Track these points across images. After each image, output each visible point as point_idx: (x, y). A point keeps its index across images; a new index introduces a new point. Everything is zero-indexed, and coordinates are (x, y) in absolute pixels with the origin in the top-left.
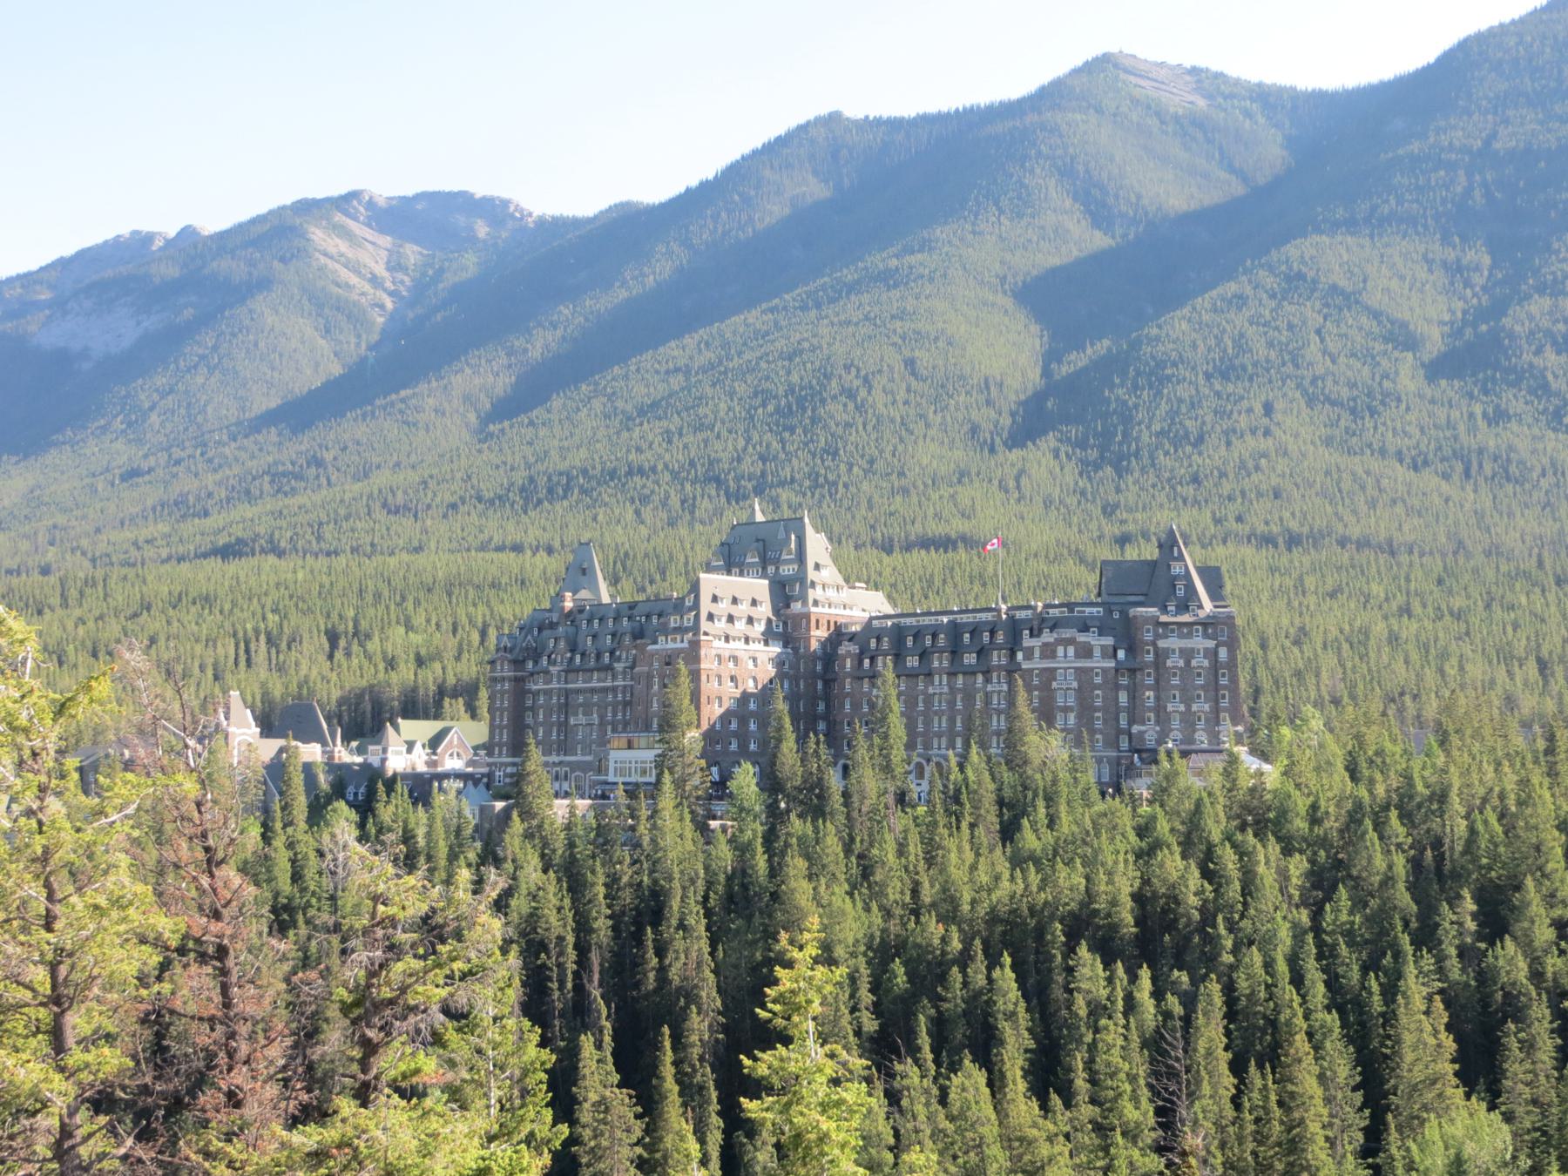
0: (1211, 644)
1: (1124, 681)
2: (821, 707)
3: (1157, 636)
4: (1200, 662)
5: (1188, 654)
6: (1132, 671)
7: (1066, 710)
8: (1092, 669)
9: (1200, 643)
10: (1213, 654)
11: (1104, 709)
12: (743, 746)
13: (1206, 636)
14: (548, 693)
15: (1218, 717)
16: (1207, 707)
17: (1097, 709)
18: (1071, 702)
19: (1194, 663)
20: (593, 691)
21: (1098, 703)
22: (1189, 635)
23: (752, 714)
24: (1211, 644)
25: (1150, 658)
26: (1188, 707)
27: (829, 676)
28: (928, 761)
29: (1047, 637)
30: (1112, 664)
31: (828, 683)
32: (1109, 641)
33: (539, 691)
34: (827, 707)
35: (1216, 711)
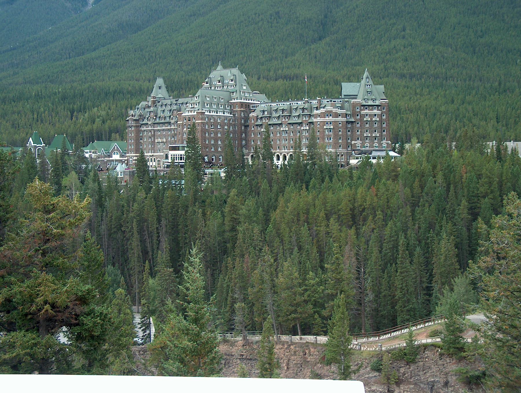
0: (379, 112)
1: (349, 126)
2: (244, 135)
3: (361, 110)
9: (375, 111)
10: (381, 116)
12: (216, 149)
14: (147, 131)
15: (382, 138)
16: (378, 135)
18: (331, 133)
20: (163, 130)
24: (379, 112)
26: (371, 134)
28: (281, 154)
29: (322, 110)
30: (344, 119)
31: (246, 126)
33: (145, 130)
35: (381, 135)
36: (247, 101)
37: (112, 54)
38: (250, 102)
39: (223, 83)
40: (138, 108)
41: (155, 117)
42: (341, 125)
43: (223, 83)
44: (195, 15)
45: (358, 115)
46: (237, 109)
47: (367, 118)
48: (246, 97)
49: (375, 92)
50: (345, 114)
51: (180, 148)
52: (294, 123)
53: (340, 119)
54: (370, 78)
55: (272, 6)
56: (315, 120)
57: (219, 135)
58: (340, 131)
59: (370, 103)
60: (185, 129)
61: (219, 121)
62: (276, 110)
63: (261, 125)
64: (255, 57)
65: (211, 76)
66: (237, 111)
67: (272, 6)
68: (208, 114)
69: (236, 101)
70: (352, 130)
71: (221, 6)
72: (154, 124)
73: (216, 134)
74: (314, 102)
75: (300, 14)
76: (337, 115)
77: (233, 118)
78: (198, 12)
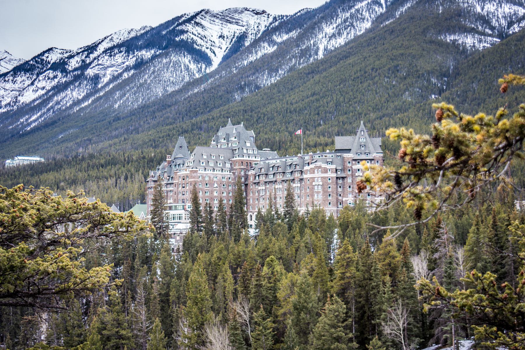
1: (340, 181)
3: (352, 164)
7: (318, 193)
8: (327, 177)
25: (350, 173)
27: (246, 183)
29: (312, 166)
30: (334, 175)
31: (246, 185)
32: (334, 167)
34: (246, 194)
36: (250, 159)
37: (222, 116)
38: (254, 159)
39: (228, 141)
40: (158, 169)
41: (168, 178)
42: (330, 181)
43: (228, 141)
44: (313, 72)
45: (349, 170)
46: (237, 167)
48: (249, 154)
49: (370, 145)
50: (335, 170)
51: (173, 208)
52: (287, 180)
53: (330, 175)
54: (365, 131)
55: (391, 59)
56: (305, 176)
57: (215, 194)
58: (329, 187)
59: (363, 157)
60: (180, 188)
61: (215, 179)
62: (273, 167)
63: (259, 183)
64: (365, 115)
65: (220, 134)
66: (236, 169)
67: (391, 59)
68: (203, 172)
69: (237, 158)
70: (343, 186)
71: (341, 62)
72: (167, 184)
73: (212, 192)
74: (307, 158)
75: (421, 67)
76: (325, 171)
77: (232, 176)
78: (317, 70)
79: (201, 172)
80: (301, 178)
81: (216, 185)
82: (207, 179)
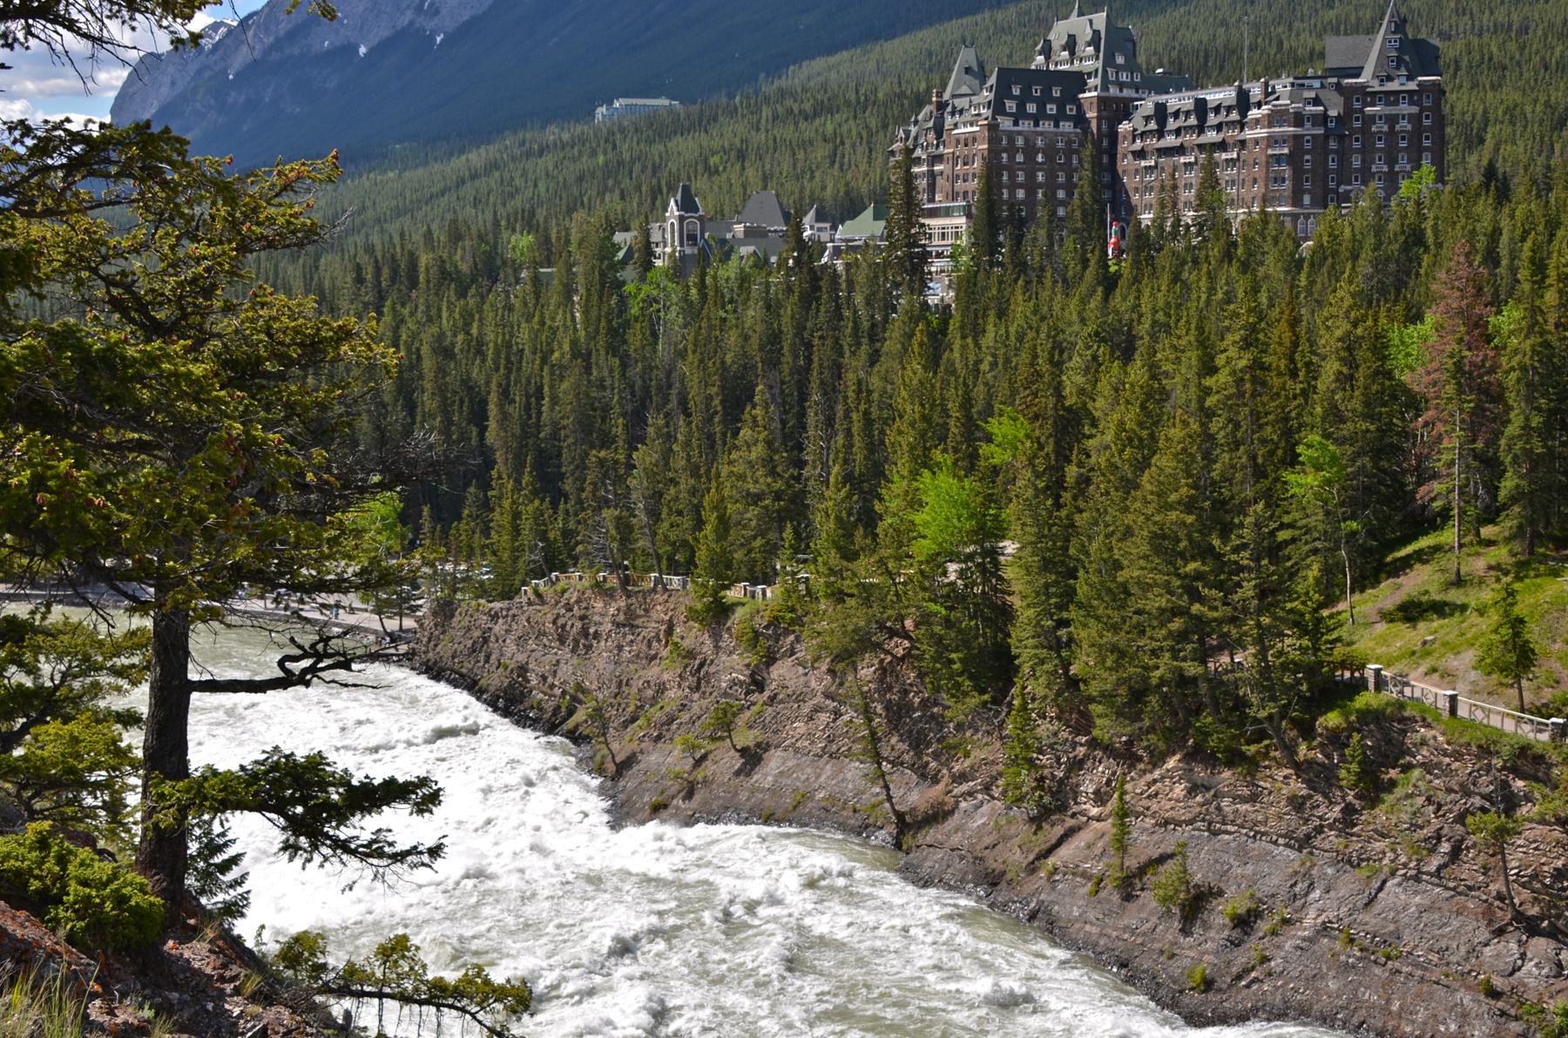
0: (1414, 109)
3: (1366, 104)
4: (1404, 125)
5: (1392, 120)
6: (1341, 138)
9: (1405, 108)
10: (1415, 119)
11: (1312, 171)
13: (1411, 103)
17: (1307, 171)
19: (1397, 128)
21: (1308, 166)
22: (1396, 103)
23: (1040, 186)
24: (1414, 109)
29: (1265, 109)
39: (1072, 53)
43: (1072, 53)
47: (1380, 127)
53: (1309, 130)
73: (1031, 176)
79: (1006, 124)
80: (1241, 137)
81: (1040, 158)
82: (1020, 142)
